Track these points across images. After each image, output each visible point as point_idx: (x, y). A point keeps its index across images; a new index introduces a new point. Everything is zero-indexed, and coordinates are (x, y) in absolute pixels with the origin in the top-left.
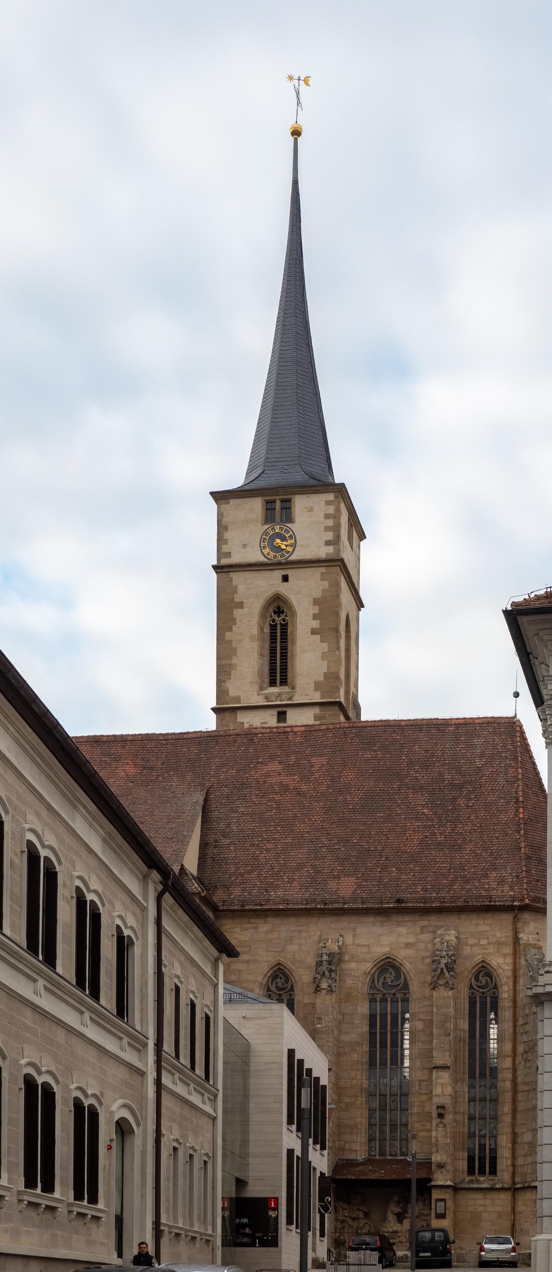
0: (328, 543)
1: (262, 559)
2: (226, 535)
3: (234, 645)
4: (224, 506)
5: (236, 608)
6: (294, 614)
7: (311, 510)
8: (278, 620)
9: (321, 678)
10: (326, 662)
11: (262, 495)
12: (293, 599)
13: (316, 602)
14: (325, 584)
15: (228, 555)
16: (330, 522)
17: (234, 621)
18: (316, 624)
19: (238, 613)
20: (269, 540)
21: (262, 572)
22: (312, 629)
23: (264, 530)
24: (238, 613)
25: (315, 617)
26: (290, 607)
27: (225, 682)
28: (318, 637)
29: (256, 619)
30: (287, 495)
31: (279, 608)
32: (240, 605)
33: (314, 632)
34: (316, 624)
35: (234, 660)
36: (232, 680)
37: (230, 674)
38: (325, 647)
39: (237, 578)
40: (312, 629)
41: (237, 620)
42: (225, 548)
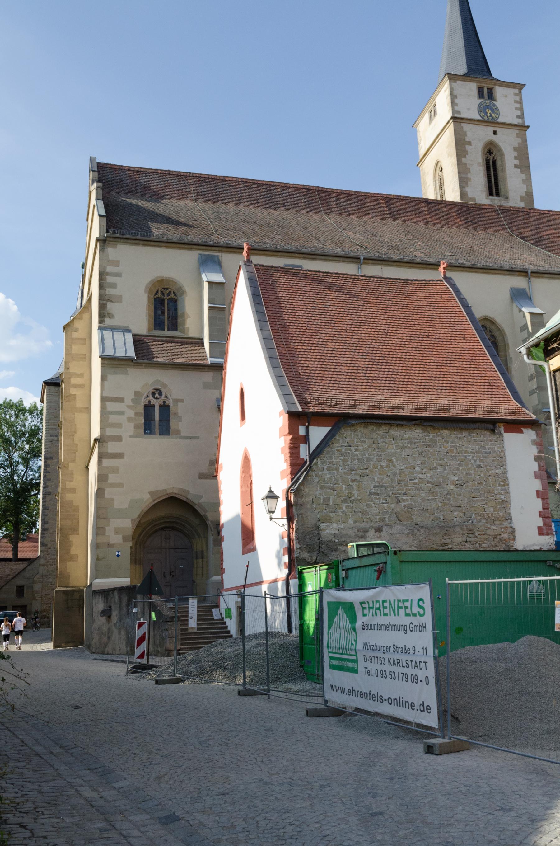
0: (518, 117)
1: (480, 118)
2: (457, 101)
3: (468, 167)
4: (453, 84)
6: (502, 154)
7: (506, 96)
8: (491, 158)
9: (524, 195)
11: (477, 82)
12: (503, 146)
13: (515, 149)
14: (519, 140)
15: (459, 112)
16: (518, 105)
17: (466, 152)
18: (517, 162)
19: (468, 148)
20: (482, 109)
24: (468, 148)
25: (516, 158)
26: (500, 150)
28: (519, 170)
30: (491, 85)
31: (490, 151)
32: (469, 143)
33: (516, 166)
34: (517, 162)
35: (469, 176)
37: (467, 184)
38: (524, 176)
39: (466, 127)
42: (456, 108)
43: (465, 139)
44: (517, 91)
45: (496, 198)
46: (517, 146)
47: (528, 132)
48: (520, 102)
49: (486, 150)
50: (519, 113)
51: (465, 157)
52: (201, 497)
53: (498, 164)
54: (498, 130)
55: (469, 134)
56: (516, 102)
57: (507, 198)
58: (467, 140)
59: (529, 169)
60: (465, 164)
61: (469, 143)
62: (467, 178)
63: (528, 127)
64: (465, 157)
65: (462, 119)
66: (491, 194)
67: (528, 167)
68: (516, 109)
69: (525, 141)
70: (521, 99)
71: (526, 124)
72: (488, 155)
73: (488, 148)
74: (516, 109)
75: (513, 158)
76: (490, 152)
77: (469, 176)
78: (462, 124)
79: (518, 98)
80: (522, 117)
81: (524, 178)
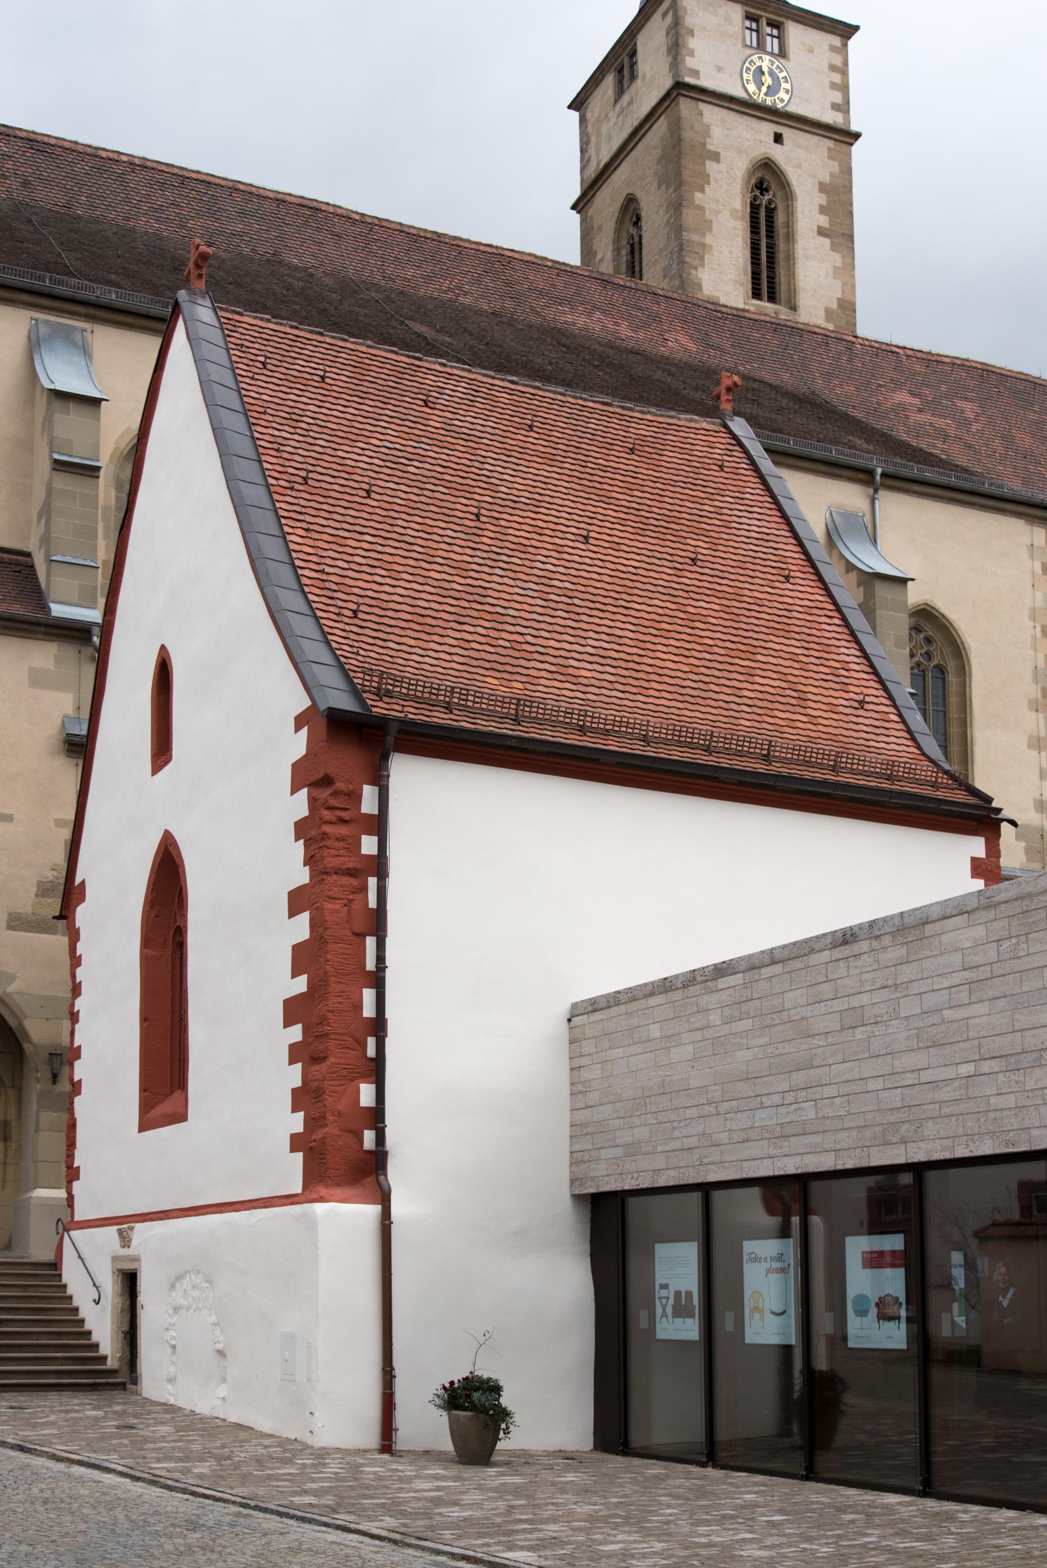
0: (835, 107)
3: (708, 216)
5: (710, 159)
7: (811, 51)
10: (839, 283)
12: (792, 174)
13: (823, 188)
16: (837, 78)
18: (824, 221)
19: (711, 167)
21: (745, 117)
22: (819, 227)
23: (746, 55)
25: (823, 210)
27: (696, 268)
29: (739, 187)
30: (779, 15)
32: (716, 157)
33: (821, 232)
34: (824, 221)
36: (706, 269)
37: (702, 259)
38: (837, 258)
40: (819, 227)
41: (712, 179)
43: (704, 144)
44: (836, 41)
45: (768, 305)
46: (827, 180)
47: (857, 148)
48: (843, 70)
49: (753, 181)
50: (837, 97)
51: (702, 190)
52: (12, 978)
53: (780, 218)
54: (786, 132)
55: (716, 131)
56: (833, 68)
57: (794, 308)
58: (710, 147)
59: (852, 242)
60: (701, 208)
61: (716, 157)
62: (704, 245)
63: (857, 136)
64: (702, 190)
65: (703, 91)
66: (756, 294)
67: (850, 238)
68: (833, 86)
69: (847, 171)
70: (846, 63)
71: (854, 127)
72: (758, 193)
73: (759, 175)
74: (833, 86)
75: (817, 208)
76: (761, 187)
77: (708, 239)
78: (702, 106)
79: (838, 61)
80: (844, 107)
81: (839, 264)
